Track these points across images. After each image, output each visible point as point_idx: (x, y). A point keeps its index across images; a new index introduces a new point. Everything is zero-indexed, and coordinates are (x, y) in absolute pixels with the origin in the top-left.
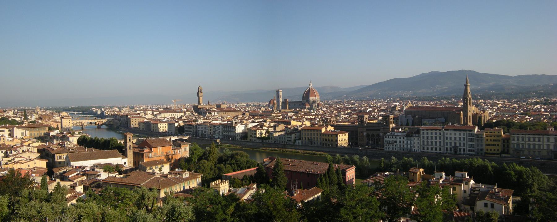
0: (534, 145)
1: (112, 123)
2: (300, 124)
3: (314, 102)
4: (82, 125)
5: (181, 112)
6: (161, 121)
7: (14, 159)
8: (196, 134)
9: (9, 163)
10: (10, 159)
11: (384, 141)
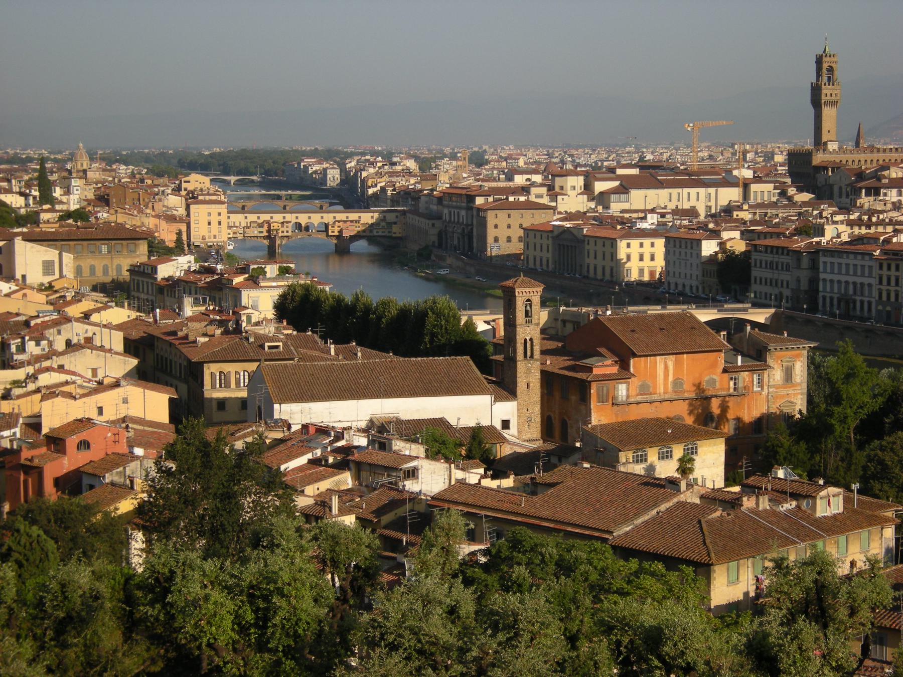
1: (397, 230)
4: (271, 237)
6: (628, 228)
7: (34, 377)
8: (810, 296)
9: (17, 391)
10: (19, 374)
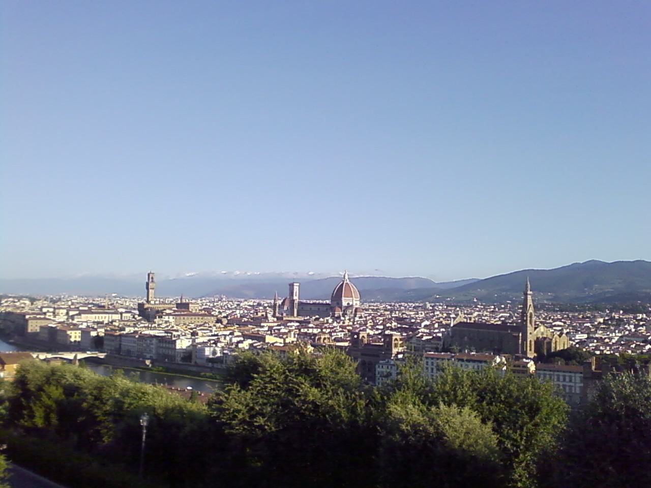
0: (564, 386)
2: (282, 341)
3: (349, 306)
5: (116, 313)
6: (75, 327)
8: (119, 350)
11: (377, 373)
